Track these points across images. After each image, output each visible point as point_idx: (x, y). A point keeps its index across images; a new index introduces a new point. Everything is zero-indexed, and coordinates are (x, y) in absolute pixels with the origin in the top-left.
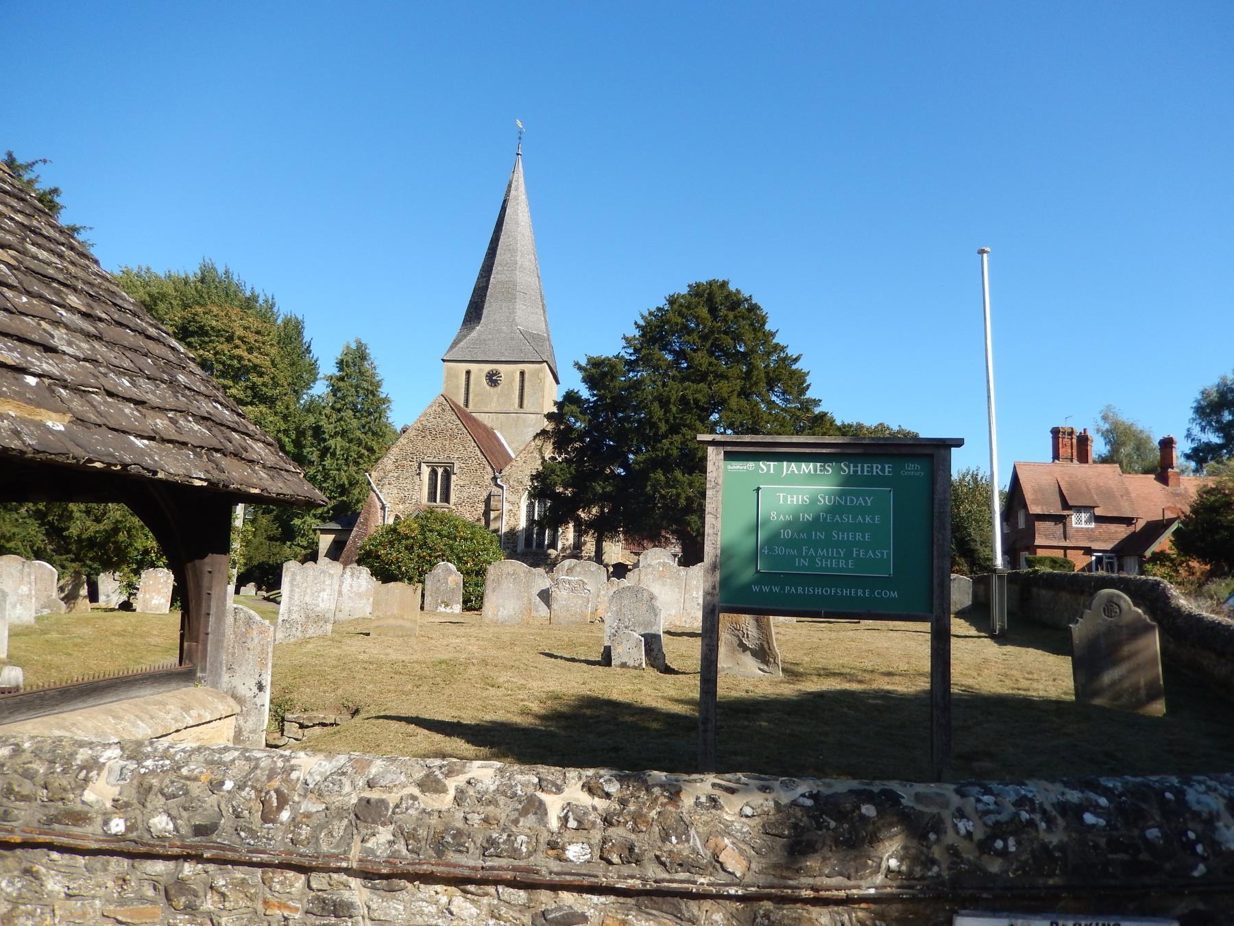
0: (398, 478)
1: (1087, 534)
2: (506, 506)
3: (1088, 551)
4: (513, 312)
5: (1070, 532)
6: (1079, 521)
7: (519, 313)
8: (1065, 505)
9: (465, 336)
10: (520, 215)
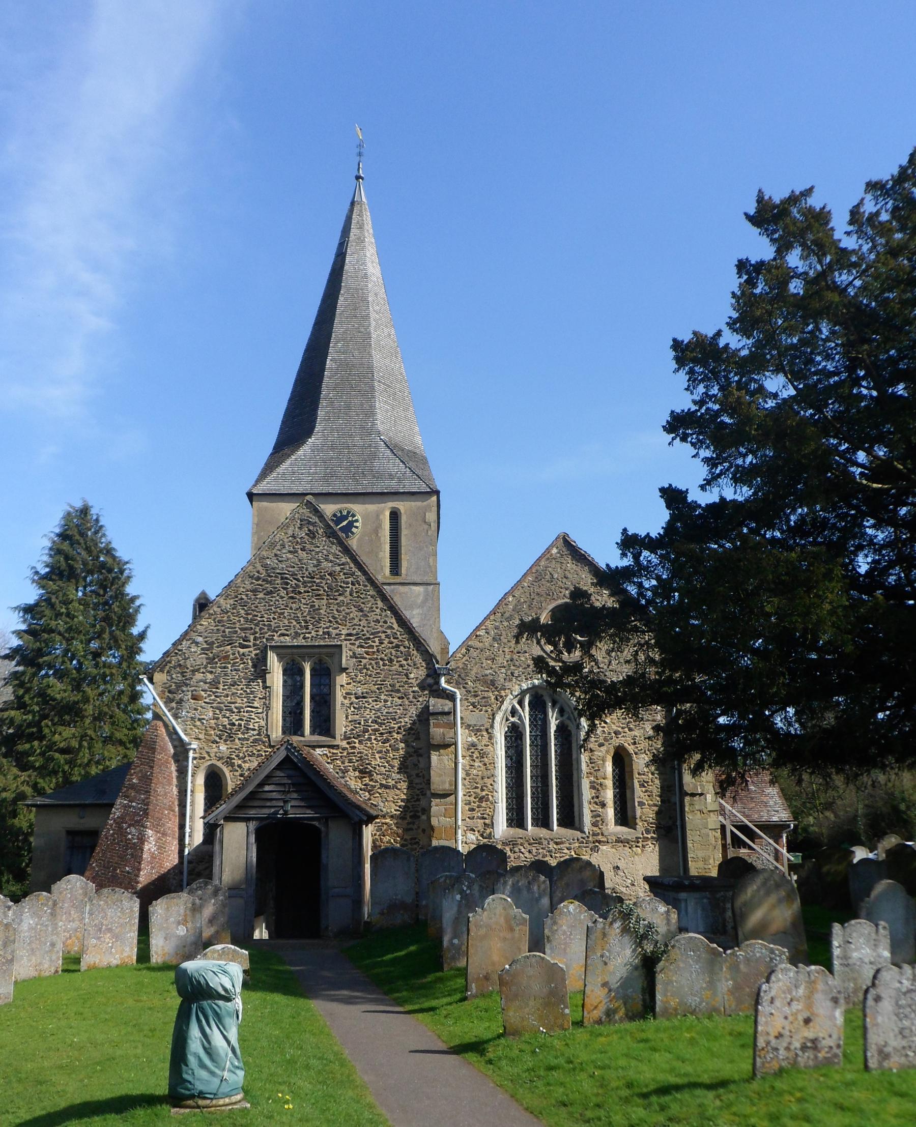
0: (215, 684)
2: (462, 736)
4: (370, 413)
7: (379, 416)
9: (289, 456)
10: (368, 263)
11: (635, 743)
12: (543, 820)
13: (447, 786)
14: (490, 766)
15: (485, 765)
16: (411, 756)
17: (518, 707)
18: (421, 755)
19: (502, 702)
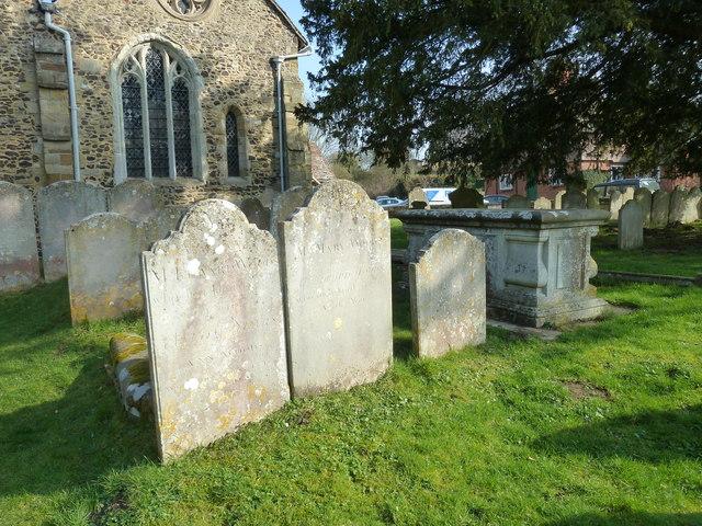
11: (246, 104)
12: (161, 169)
13: (62, 133)
14: (107, 116)
15: (103, 114)
16: (15, 99)
17: (134, 59)
18: (27, 99)
19: (119, 51)
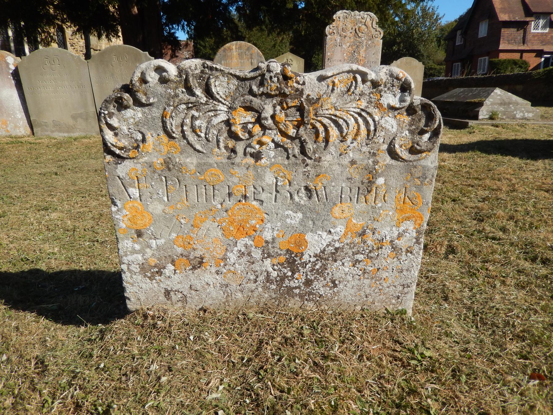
1: (541, 38)
3: (539, 53)
5: (529, 37)
6: (536, 27)
8: (528, 12)
